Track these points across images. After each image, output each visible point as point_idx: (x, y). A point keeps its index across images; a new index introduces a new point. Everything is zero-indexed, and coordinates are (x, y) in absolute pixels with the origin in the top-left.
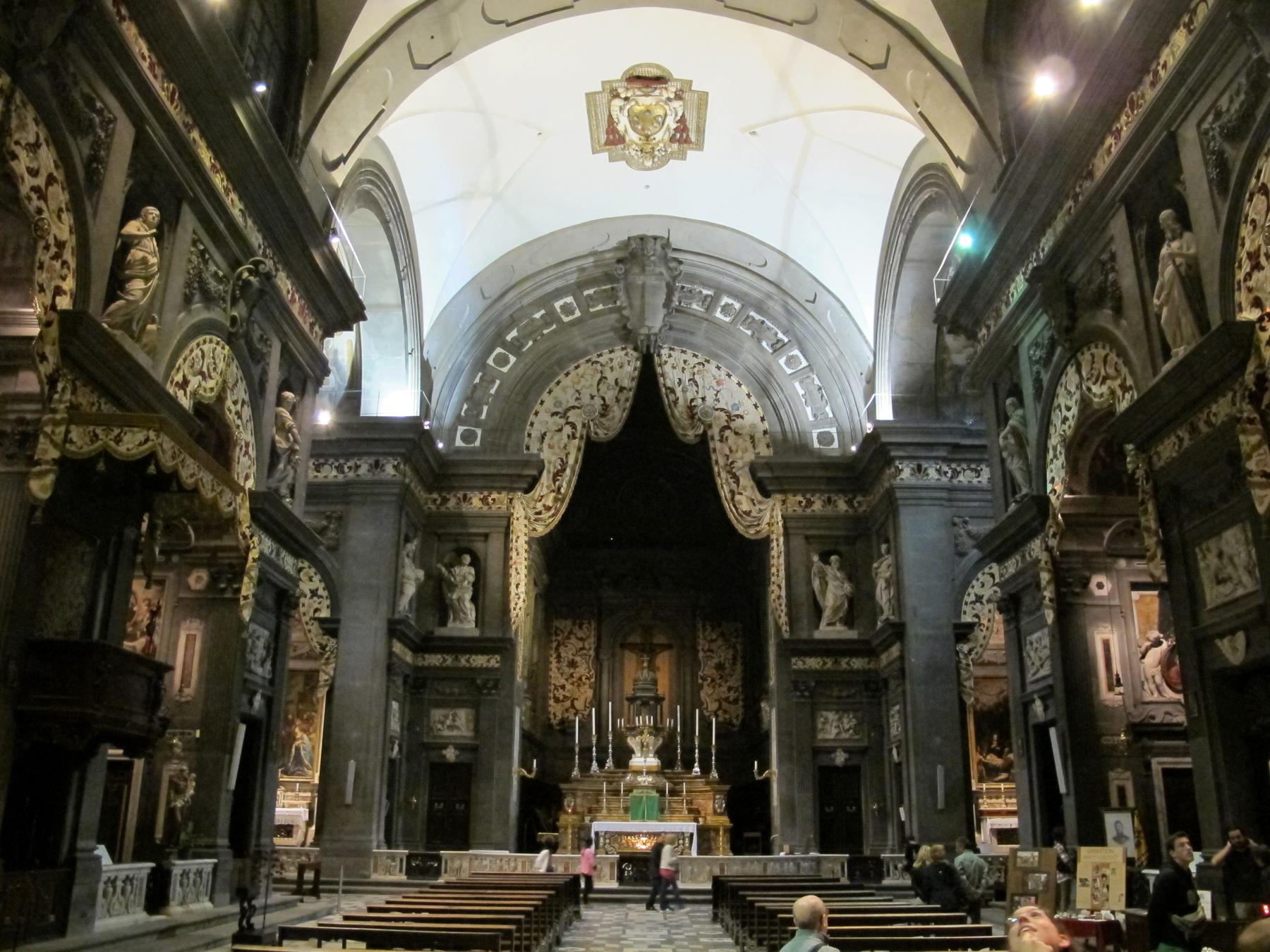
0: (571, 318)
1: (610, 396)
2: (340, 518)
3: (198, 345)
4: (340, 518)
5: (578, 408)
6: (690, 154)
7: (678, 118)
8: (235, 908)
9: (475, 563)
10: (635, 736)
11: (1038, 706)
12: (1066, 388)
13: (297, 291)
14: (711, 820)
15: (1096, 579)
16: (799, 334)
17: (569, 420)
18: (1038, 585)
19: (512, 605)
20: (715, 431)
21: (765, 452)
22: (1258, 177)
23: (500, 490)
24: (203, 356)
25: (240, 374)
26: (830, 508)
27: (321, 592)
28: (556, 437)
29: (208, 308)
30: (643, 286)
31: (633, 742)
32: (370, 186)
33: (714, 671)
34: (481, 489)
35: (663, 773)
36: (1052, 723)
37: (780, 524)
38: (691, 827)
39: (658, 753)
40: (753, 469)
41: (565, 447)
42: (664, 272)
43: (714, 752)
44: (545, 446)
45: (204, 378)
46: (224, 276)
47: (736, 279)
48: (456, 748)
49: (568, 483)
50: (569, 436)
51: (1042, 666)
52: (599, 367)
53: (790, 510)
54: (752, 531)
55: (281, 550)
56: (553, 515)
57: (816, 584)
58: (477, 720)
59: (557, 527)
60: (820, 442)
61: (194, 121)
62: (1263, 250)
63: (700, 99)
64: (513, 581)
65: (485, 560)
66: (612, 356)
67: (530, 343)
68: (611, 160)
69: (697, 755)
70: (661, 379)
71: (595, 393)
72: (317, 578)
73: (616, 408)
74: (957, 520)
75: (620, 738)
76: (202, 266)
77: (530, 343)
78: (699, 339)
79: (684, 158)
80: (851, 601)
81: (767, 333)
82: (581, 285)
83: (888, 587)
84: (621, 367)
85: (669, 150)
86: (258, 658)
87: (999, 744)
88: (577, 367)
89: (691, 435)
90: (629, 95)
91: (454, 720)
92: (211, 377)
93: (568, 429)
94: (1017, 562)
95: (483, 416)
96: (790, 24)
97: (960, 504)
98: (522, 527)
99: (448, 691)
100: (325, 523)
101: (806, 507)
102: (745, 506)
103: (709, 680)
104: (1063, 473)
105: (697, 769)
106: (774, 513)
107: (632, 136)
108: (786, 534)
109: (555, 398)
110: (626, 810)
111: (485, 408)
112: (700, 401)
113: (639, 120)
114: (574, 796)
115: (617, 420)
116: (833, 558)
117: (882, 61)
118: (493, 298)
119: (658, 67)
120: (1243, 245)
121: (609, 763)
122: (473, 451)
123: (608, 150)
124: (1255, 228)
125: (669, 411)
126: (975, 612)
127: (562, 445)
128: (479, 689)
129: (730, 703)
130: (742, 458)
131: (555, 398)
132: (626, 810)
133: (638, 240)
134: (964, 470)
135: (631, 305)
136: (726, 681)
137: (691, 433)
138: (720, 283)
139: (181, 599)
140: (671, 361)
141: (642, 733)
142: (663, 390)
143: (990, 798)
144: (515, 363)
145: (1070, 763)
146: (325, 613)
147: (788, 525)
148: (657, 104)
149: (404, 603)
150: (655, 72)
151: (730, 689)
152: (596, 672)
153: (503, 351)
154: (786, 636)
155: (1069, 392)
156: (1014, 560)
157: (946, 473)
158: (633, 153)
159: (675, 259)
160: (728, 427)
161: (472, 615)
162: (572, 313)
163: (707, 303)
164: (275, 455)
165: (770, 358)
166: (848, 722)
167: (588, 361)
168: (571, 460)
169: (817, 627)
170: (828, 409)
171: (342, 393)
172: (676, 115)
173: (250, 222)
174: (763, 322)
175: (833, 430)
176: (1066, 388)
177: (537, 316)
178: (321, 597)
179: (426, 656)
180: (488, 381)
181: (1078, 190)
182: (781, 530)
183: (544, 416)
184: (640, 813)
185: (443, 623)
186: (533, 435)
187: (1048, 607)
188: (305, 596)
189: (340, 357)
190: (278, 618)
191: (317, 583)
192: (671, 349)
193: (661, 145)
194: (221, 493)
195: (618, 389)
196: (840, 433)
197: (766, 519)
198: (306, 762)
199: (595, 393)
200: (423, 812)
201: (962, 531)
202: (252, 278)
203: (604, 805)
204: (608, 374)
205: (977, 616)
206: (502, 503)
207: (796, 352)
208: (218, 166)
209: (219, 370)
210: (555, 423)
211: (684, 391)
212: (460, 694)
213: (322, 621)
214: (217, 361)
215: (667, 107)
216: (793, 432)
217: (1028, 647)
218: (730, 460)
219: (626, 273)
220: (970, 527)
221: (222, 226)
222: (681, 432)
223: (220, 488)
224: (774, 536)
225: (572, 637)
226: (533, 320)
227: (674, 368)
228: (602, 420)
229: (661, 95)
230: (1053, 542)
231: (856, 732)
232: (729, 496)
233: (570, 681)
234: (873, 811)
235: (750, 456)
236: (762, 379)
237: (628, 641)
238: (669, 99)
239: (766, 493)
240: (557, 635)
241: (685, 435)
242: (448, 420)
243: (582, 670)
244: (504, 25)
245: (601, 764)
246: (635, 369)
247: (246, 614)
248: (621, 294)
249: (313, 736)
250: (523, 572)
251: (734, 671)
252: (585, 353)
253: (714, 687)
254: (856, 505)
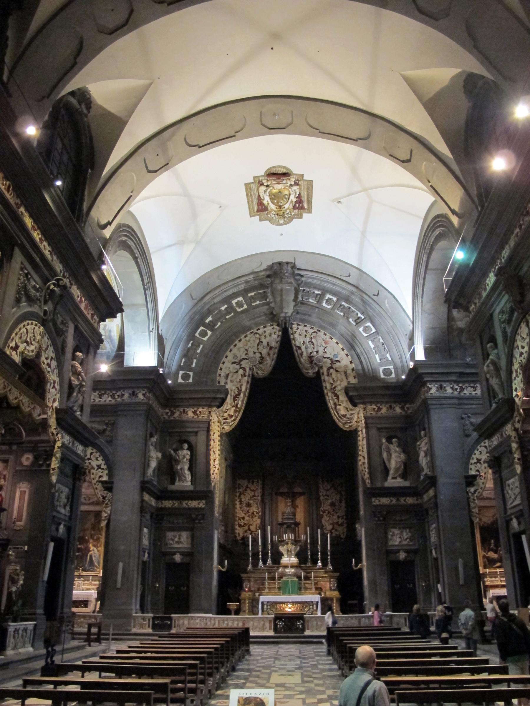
0: (242, 309)
1: (264, 352)
2: (113, 424)
3: (24, 326)
4: (113, 424)
5: (247, 359)
6: (305, 215)
7: (297, 195)
8: (44, 651)
9: (191, 448)
10: (283, 546)
11: (514, 523)
12: (521, 336)
13: (84, 296)
14: (329, 594)
16: (370, 314)
17: (242, 366)
18: (511, 452)
19: (212, 472)
20: (325, 370)
21: (353, 381)
23: (203, 406)
24: (27, 333)
25: (50, 342)
26: (391, 411)
27: (103, 466)
28: (235, 376)
29: (30, 306)
30: (282, 290)
31: (282, 549)
32: (126, 238)
33: (329, 507)
34: (193, 406)
35: (300, 567)
36: (523, 532)
37: (363, 421)
38: (317, 598)
39: (297, 555)
40: (347, 391)
41: (240, 382)
42: (293, 282)
43: (329, 554)
44: (229, 381)
45: (28, 345)
46: (40, 287)
47: (334, 285)
48: (181, 554)
49: (241, 402)
50: (242, 375)
51: (515, 498)
52: (258, 336)
53: (368, 413)
54: (347, 426)
55: (75, 442)
56: (234, 420)
57: (385, 455)
58: (193, 537)
59: (236, 426)
60: (384, 374)
61: (22, 201)
63: (308, 184)
64: (212, 458)
65: (196, 446)
66: (265, 329)
67: (219, 324)
68: (261, 220)
69: (319, 556)
70: (293, 342)
71: (256, 350)
72: (100, 459)
73: (268, 359)
74: (464, 416)
75: (275, 546)
76: (26, 282)
77: (219, 324)
78: (314, 319)
79: (301, 218)
80: (405, 464)
81: (352, 314)
82: (246, 291)
83: (426, 455)
84: (270, 335)
85: (293, 213)
86: (62, 504)
87: (495, 546)
88: (246, 336)
89: (311, 373)
90: (269, 184)
91: (179, 538)
92: (32, 344)
93: (241, 372)
94: (498, 438)
95: (194, 366)
96: (356, 140)
97: (465, 407)
98: (216, 427)
99: (175, 521)
100: (105, 427)
101: (378, 411)
102: (343, 412)
103: (327, 512)
104: (522, 385)
105: (320, 564)
106: (360, 415)
107: (272, 206)
108: (367, 427)
109: (234, 354)
110: (279, 588)
111: (195, 361)
112: (315, 353)
113: (275, 197)
114: (249, 581)
115: (269, 365)
116: (394, 440)
117: (409, 158)
118: (198, 299)
119: (284, 167)
121: (269, 561)
122: (188, 385)
123: (259, 215)
125: (298, 360)
126: (477, 468)
127: (238, 380)
128: (193, 520)
129: (339, 525)
130: (340, 385)
131: (234, 354)
132: (279, 588)
133: (278, 265)
134: (467, 387)
135: (275, 302)
136: (336, 513)
137: (310, 371)
138: (325, 287)
139: (17, 470)
140: (298, 331)
141: (287, 544)
142: (295, 348)
143: (491, 577)
144: (211, 336)
146: (105, 478)
147: (368, 422)
148: (284, 188)
149: (150, 472)
150: (283, 171)
151: (339, 517)
152: (262, 509)
153: (204, 329)
154: (369, 486)
155: (523, 338)
156: (496, 437)
157: (456, 389)
158: (273, 216)
159: (299, 275)
160: (331, 368)
161: (189, 478)
162: (242, 306)
163: (317, 298)
164: (71, 388)
165: (355, 327)
166: (406, 534)
167: (252, 333)
168: (243, 389)
169: (386, 480)
170: (388, 356)
171: (114, 353)
172: (296, 194)
173: (55, 258)
174: (349, 308)
175: (392, 367)
176: (521, 336)
177: (223, 308)
178: (103, 469)
179: (163, 502)
180: (196, 345)
181: (521, 222)
182: (364, 425)
183: (227, 364)
184: (287, 589)
185: (173, 482)
186: (222, 375)
187: (517, 464)
188: (94, 469)
189: (112, 334)
190: (74, 480)
191: (101, 461)
192: (298, 325)
193: (288, 211)
194: (34, 409)
195: (269, 348)
196: (396, 368)
197: (355, 419)
198: (96, 564)
199: (256, 350)
200: (162, 592)
201: (467, 422)
202: (55, 289)
203: (267, 586)
204: (263, 339)
205: (478, 471)
206: (205, 414)
207: (369, 324)
208: (36, 227)
209: (37, 340)
210: (234, 368)
211: (306, 348)
212: (183, 523)
213: (103, 483)
214: (36, 335)
215: (290, 190)
216: (368, 369)
217: (507, 488)
218: (334, 386)
219: (272, 283)
220: (472, 420)
221: (38, 260)
222: (305, 371)
223: (33, 405)
224: (360, 429)
225: (248, 489)
226: (221, 311)
227: (300, 335)
228: (261, 365)
229: (287, 183)
230: (518, 426)
231: (411, 541)
232: (333, 406)
233: (247, 515)
234: (423, 586)
235: (345, 384)
236: (350, 340)
238: (291, 185)
239: (355, 405)
240: (239, 489)
241: (308, 373)
242: (174, 368)
243: (254, 508)
244: (197, 147)
245: (265, 562)
246: (278, 336)
247: (54, 479)
248: (270, 295)
249: (99, 549)
250: (218, 453)
251: (341, 507)
252: (250, 328)
253: (330, 517)
254: (406, 409)
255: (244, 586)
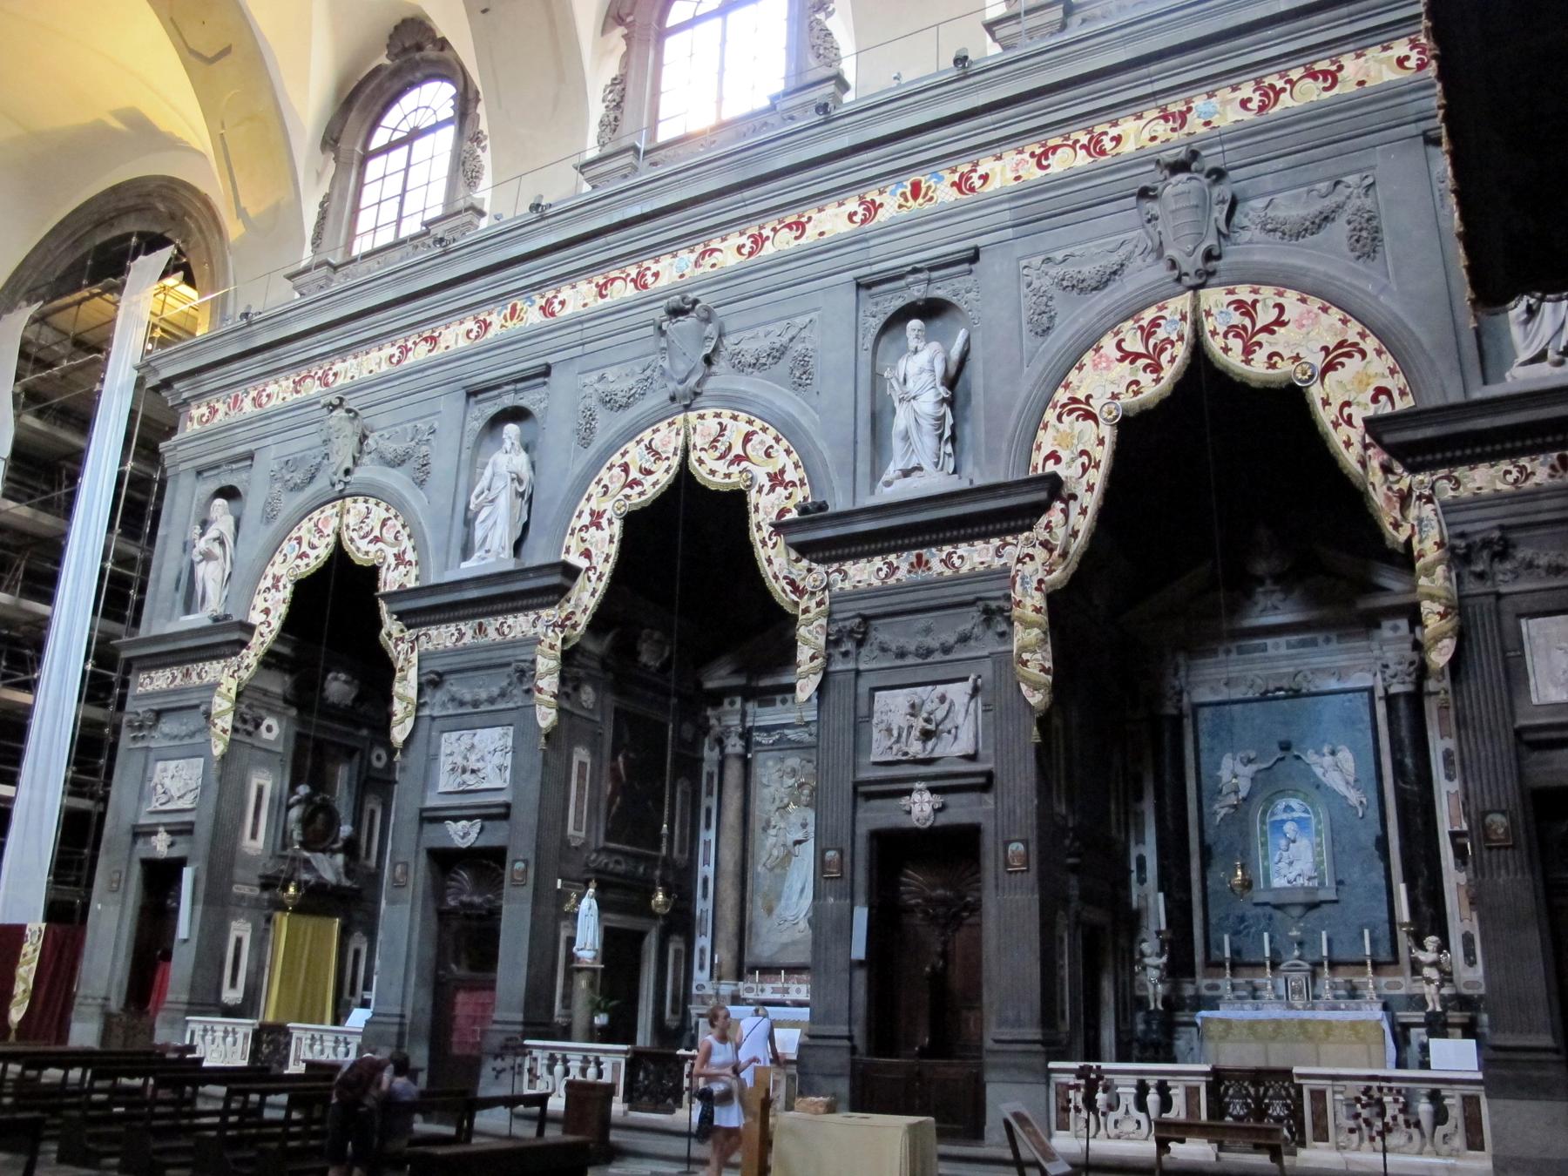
12: (316, 525)
15: (270, 721)
22: (623, 455)
62: (606, 516)
94: (174, 678)
120: (588, 500)
124: (605, 493)
145: (199, 907)
181: (410, 344)
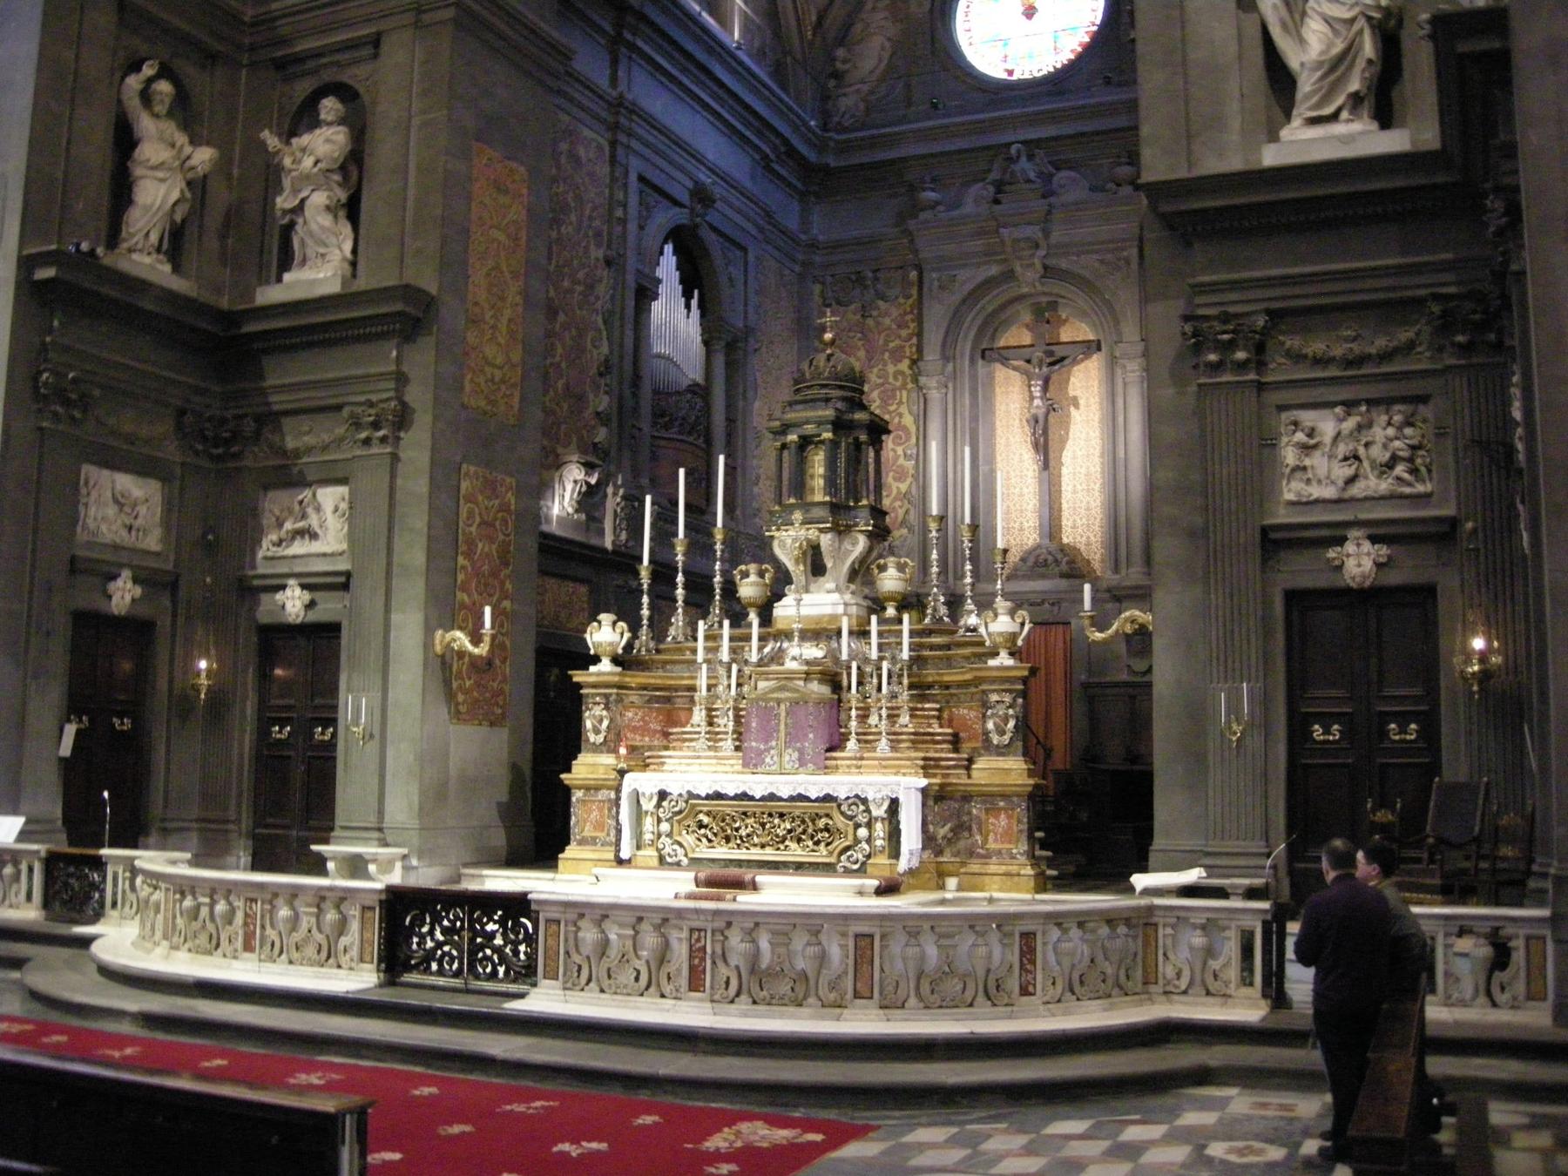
48: (304, 587)
237: (1002, 343)
255: (588, 724)
